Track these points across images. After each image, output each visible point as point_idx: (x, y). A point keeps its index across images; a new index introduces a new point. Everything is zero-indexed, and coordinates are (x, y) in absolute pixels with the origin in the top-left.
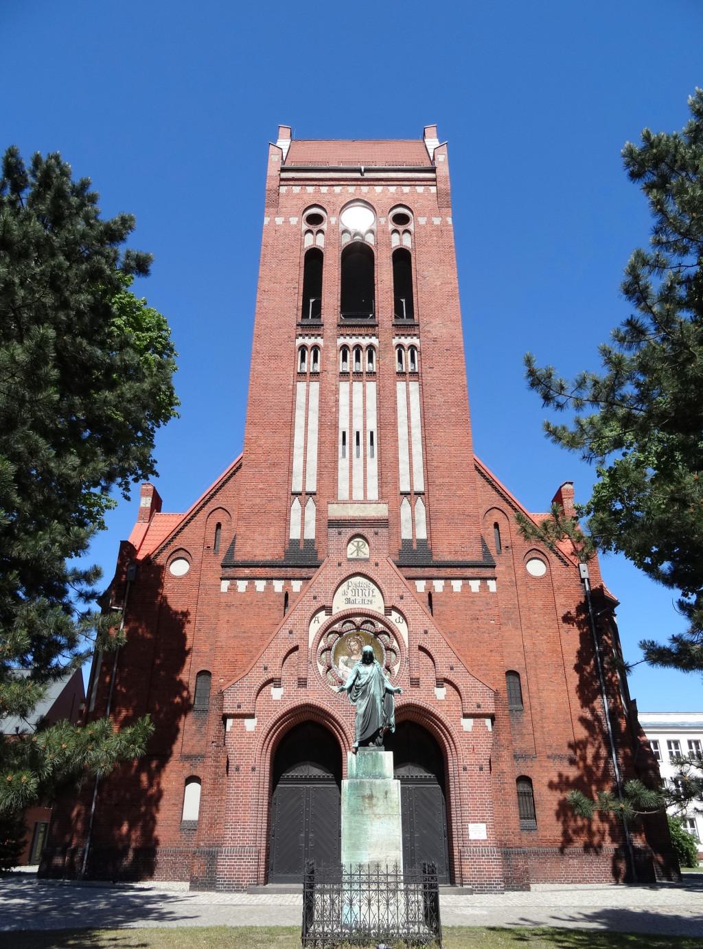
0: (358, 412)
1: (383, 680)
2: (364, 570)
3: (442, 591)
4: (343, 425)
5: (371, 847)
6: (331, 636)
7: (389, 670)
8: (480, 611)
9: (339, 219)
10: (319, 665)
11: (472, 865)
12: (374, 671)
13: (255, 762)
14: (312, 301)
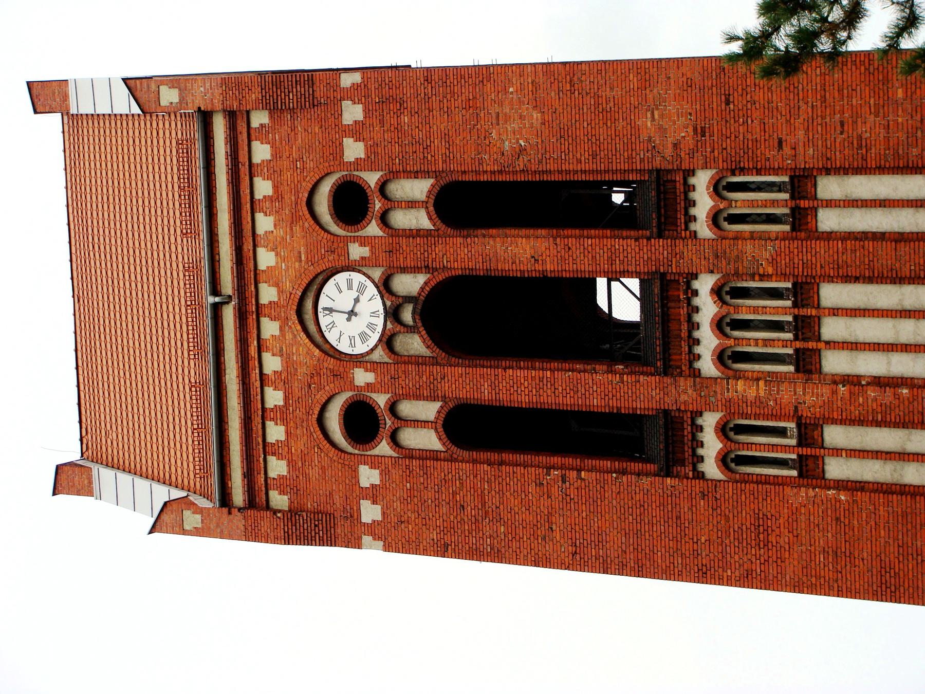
9: (358, 360)
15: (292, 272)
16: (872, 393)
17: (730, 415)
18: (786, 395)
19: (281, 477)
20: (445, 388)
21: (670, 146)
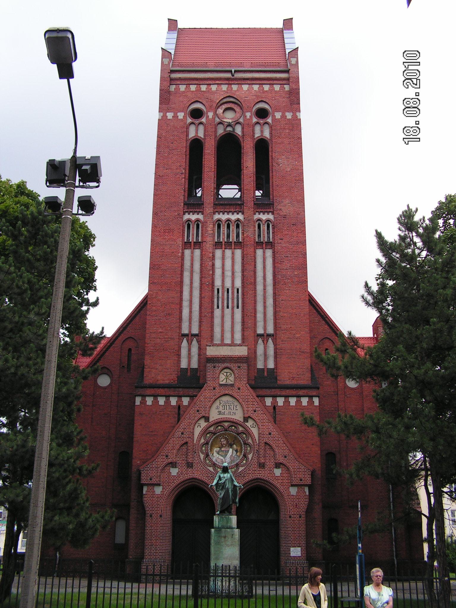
0: (228, 273)
1: (233, 481)
2: (230, 392)
3: (282, 405)
4: (218, 283)
5: (224, 559)
6: (208, 435)
7: (246, 457)
10: (201, 454)
12: (228, 476)
14: (195, 177)
16: (210, 263)
17: (203, 223)
18: (209, 239)
19: (179, 89)
20: (208, 139)
21: (281, 208)
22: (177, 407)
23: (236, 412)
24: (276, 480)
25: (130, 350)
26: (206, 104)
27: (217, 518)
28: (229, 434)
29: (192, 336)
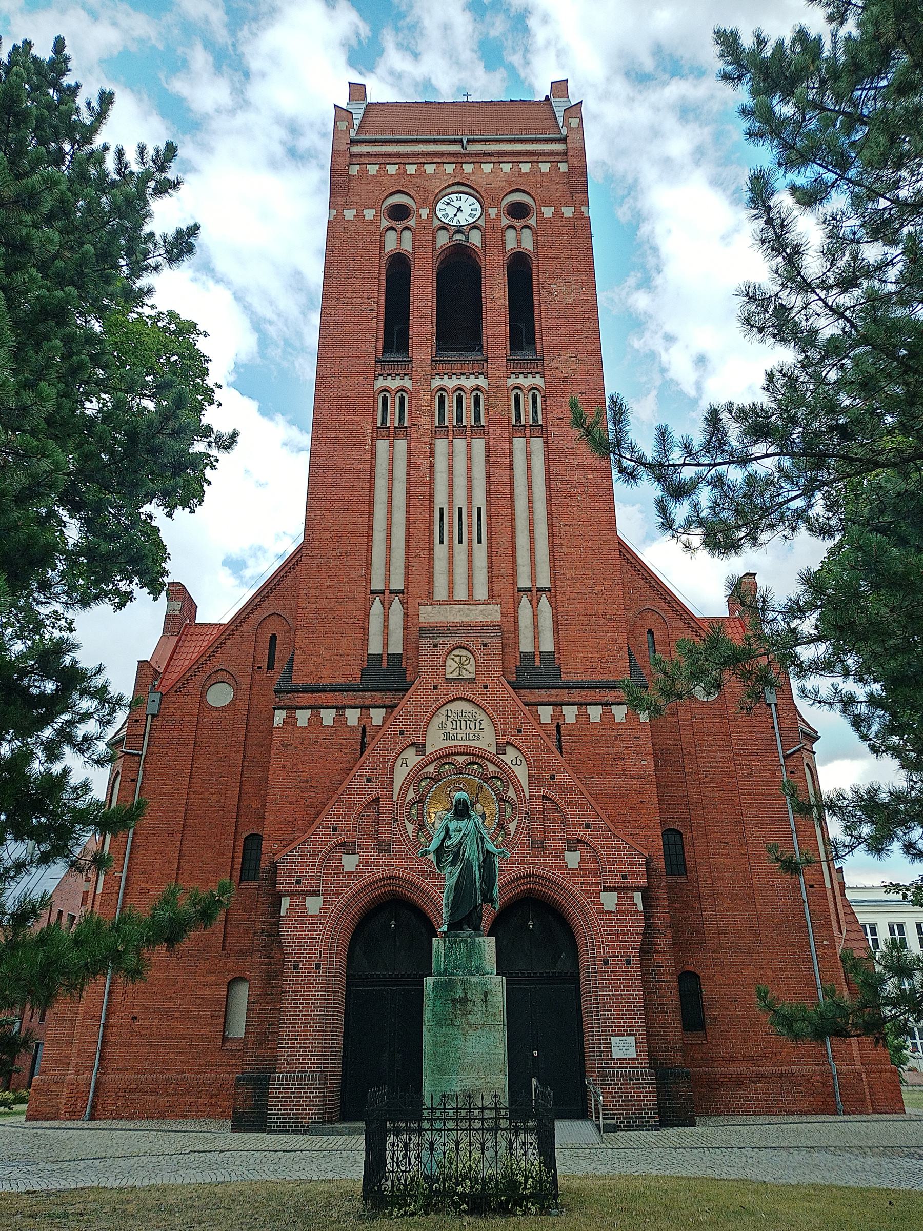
2: (468, 695)
4: (441, 499)
5: (463, 1070)
6: (423, 784)
8: (626, 748)
11: (616, 1093)
13: (320, 957)
14: (397, 328)
15: (481, 180)
20: (420, 252)
21: (557, 365)
22: (360, 728)
23: (482, 734)
24: (570, 877)
25: (273, 638)
26: (417, 197)
27: (441, 942)
28: (466, 781)
29: (390, 593)
